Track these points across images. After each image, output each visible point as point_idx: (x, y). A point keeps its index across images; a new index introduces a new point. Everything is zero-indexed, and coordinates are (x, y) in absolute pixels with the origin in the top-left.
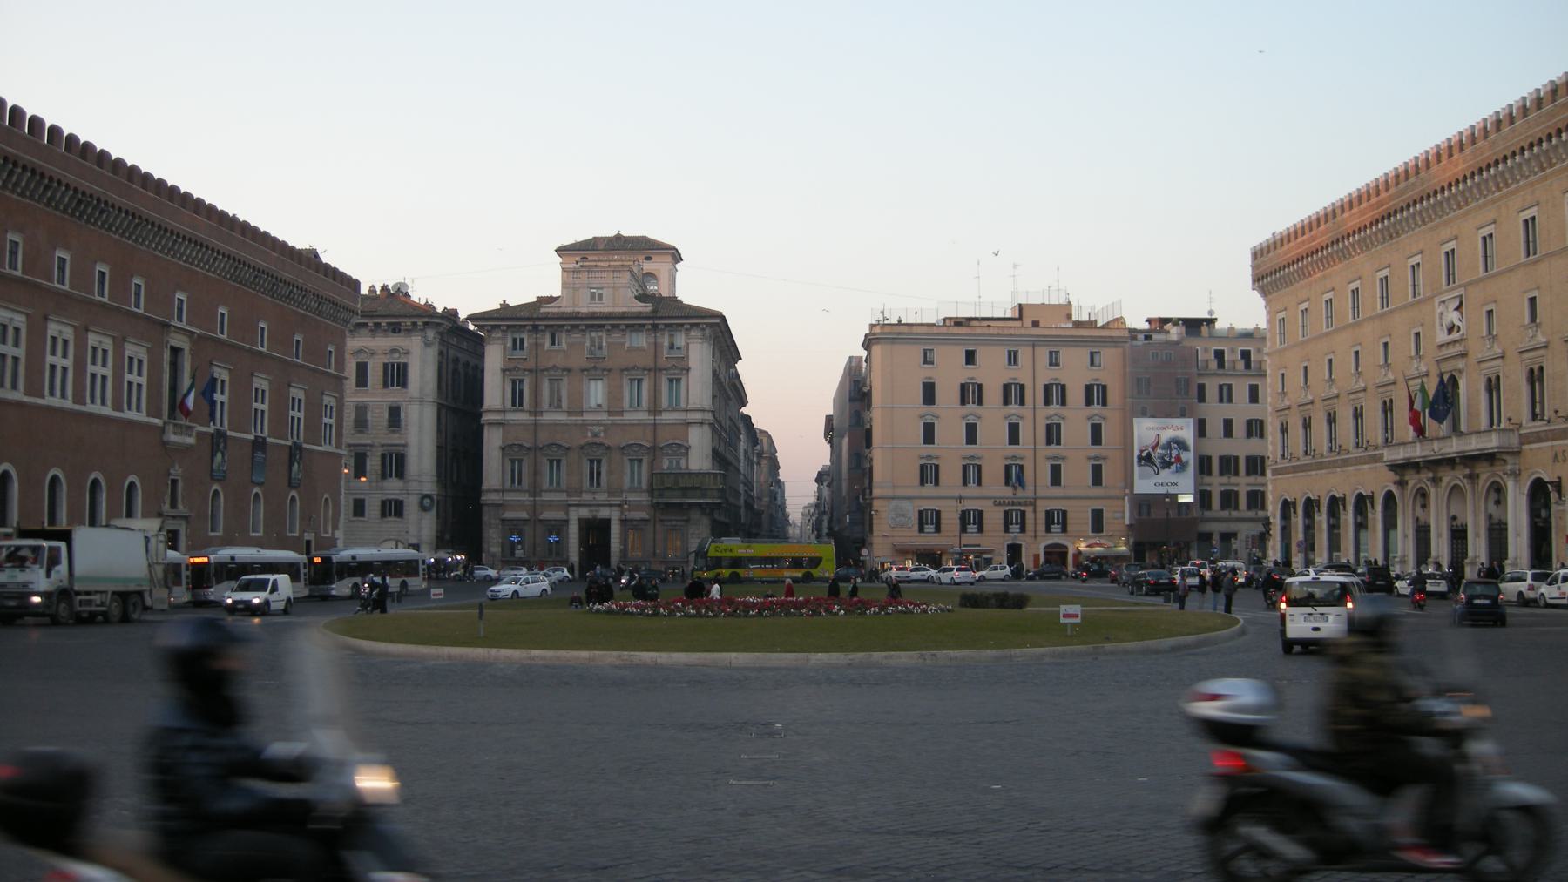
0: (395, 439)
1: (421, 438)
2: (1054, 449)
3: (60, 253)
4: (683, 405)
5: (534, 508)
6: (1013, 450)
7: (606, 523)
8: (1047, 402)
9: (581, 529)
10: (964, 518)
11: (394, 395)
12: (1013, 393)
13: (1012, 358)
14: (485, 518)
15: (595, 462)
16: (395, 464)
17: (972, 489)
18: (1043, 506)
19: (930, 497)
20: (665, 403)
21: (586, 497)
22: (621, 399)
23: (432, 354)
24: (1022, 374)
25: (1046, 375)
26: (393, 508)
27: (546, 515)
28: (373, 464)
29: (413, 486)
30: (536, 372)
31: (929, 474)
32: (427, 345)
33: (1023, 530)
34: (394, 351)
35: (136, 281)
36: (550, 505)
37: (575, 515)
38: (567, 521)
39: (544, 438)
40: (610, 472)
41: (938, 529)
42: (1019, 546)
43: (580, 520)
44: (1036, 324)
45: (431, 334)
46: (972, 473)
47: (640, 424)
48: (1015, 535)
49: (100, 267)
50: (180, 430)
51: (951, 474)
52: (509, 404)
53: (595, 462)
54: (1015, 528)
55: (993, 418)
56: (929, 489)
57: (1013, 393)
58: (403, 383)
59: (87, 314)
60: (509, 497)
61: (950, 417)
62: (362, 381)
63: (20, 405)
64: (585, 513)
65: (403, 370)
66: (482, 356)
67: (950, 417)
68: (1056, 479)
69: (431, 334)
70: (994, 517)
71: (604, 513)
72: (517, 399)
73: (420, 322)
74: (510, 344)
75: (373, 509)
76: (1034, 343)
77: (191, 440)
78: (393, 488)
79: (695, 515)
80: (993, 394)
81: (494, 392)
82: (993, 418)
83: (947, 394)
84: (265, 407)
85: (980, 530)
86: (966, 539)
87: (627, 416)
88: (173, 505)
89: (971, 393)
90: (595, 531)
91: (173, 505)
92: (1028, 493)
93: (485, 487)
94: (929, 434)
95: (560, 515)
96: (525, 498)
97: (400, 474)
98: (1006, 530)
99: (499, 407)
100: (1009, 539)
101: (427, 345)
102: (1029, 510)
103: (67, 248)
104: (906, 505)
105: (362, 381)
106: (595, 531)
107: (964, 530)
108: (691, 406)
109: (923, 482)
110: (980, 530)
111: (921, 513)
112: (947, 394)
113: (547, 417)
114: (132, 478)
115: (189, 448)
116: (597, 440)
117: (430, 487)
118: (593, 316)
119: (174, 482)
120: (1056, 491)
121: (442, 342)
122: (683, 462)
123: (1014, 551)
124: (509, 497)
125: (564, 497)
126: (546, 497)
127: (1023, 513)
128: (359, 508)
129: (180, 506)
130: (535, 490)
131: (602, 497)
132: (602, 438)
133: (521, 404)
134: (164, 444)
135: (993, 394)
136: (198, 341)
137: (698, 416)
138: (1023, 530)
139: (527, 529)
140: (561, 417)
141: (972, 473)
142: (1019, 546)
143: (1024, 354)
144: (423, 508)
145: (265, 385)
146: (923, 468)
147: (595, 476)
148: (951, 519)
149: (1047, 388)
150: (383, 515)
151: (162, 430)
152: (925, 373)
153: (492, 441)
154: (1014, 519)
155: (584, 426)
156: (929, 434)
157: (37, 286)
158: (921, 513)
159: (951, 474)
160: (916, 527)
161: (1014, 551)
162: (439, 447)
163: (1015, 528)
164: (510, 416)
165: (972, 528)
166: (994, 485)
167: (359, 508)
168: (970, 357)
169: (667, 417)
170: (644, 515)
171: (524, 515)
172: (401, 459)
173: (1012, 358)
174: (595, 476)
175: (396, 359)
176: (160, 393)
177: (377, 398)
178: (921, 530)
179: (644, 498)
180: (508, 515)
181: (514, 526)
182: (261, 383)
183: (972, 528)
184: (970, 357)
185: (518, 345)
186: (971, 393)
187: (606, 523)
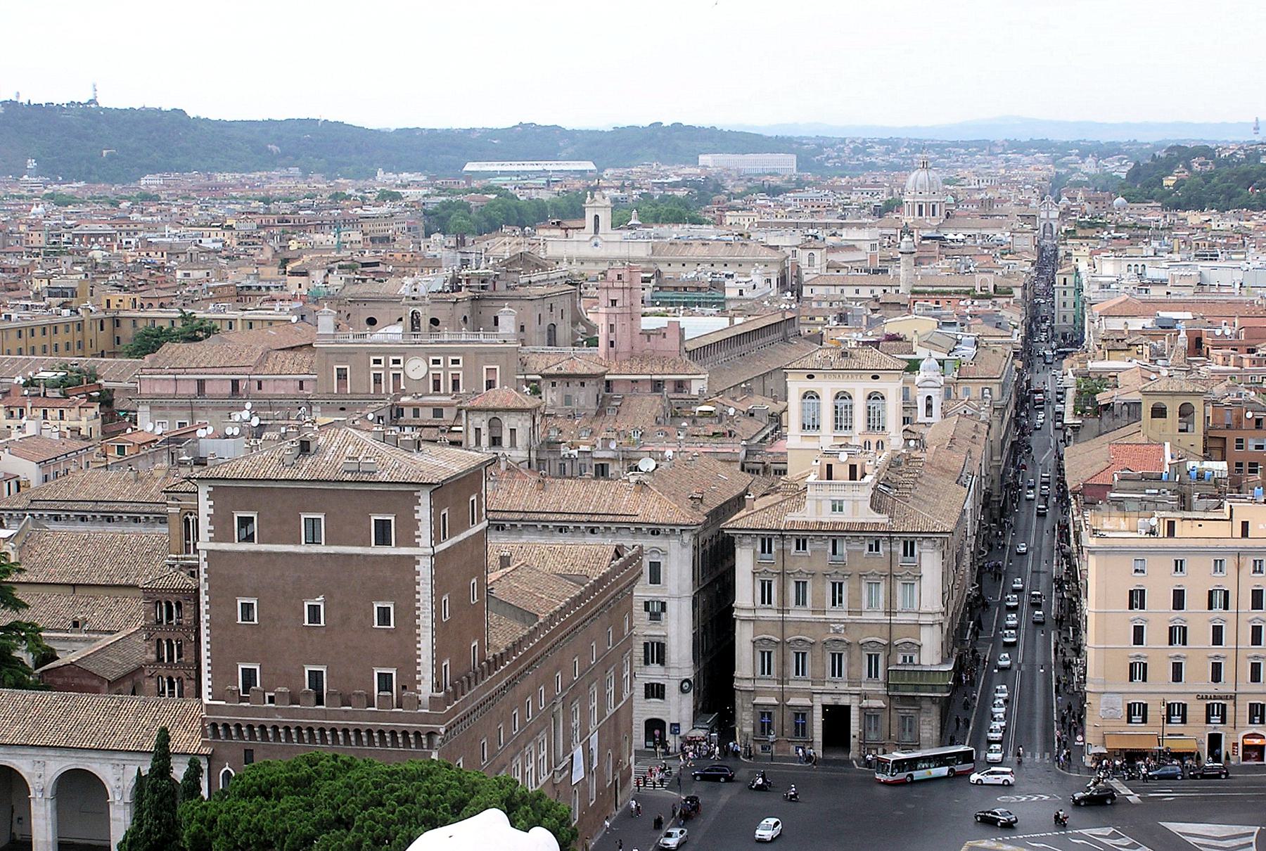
0: (654, 631)
1: (679, 631)
2: (1256, 650)
4: (916, 608)
5: (782, 696)
7: (847, 709)
9: (824, 714)
13: (1219, 565)
14: (738, 701)
15: (837, 659)
16: (656, 652)
19: (1138, 692)
21: (829, 687)
22: (860, 600)
23: (688, 554)
24: (1226, 581)
26: (654, 691)
29: (674, 673)
30: (783, 575)
31: (1138, 671)
32: (684, 546)
33: (1223, 721)
36: (796, 693)
40: (850, 665)
41: (1144, 721)
43: (824, 707)
45: (687, 537)
47: (878, 624)
48: (1216, 726)
52: (759, 601)
53: (837, 659)
54: (1216, 719)
56: (1138, 685)
57: (1218, 599)
60: (759, 684)
64: (828, 700)
67: (1158, 615)
68: (1256, 676)
69: (687, 537)
70: (1196, 710)
71: (844, 701)
72: (766, 597)
73: (678, 530)
74: (759, 549)
78: (654, 673)
79: (926, 705)
81: (745, 593)
82: (1198, 619)
85: (1184, 721)
86: (1170, 728)
87: (864, 616)
90: (837, 718)
92: (1225, 687)
93: (737, 674)
95: (806, 702)
96: (775, 685)
97: (661, 661)
98: (1208, 721)
99: (751, 605)
101: (684, 546)
102: (1229, 703)
104: (1119, 698)
106: (837, 718)
108: (923, 609)
110: (1184, 721)
111: (1129, 705)
113: (792, 615)
116: (837, 637)
117: (689, 674)
120: (1256, 687)
121: (696, 536)
122: (915, 660)
123: (1215, 740)
124: (759, 684)
125: (809, 685)
126: (792, 685)
127: (1224, 706)
131: (843, 687)
133: (770, 602)
137: (929, 619)
138: (1223, 721)
139: (777, 716)
140: (808, 616)
143: (1229, 563)
144: (683, 691)
147: (837, 670)
148: (1156, 711)
150: (647, 697)
152: (1135, 582)
153: (744, 637)
154: (1216, 710)
155: (826, 623)
158: (1129, 705)
161: (1215, 740)
163: (1216, 719)
164: (759, 613)
166: (1197, 680)
168: (1179, 566)
169: (899, 618)
170: (881, 704)
171: (774, 701)
172: (661, 648)
174: (837, 670)
178: (1129, 721)
179: (882, 689)
180: (759, 700)
181: (765, 718)
184: (1179, 566)
185: (766, 546)
187: (847, 709)
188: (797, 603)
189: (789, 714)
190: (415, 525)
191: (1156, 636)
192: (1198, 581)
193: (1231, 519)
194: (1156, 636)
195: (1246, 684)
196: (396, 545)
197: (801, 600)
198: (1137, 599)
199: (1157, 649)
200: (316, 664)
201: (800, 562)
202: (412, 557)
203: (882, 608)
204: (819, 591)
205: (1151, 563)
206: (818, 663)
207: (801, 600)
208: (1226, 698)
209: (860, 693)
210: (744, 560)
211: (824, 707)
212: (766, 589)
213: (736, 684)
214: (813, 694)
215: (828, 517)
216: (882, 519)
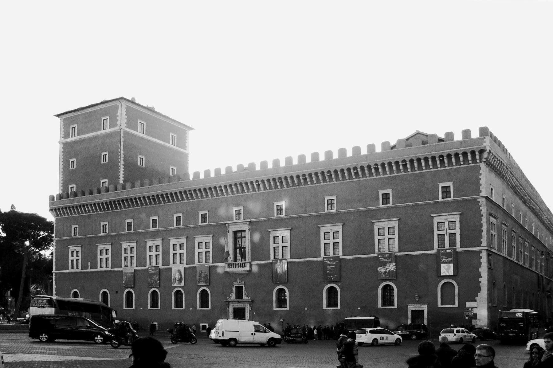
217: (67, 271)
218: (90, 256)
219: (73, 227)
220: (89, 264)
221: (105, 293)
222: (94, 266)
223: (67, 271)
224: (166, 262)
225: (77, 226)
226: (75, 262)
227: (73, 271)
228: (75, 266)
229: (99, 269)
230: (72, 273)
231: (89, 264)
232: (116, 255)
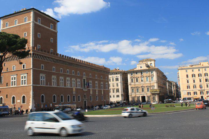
0: (118, 87)
3: (67, 70)
6: (194, 83)
8: (205, 76)
10: (194, 93)
11: (117, 82)
12: (200, 75)
13: (199, 70)
16: (118, 91)
17: (195, 89)
18: (206, 91)
19: (189, 90)
20: (151, 80)
21: (142, 93)
24: (201, 72)
25: (204, 72)
26: (118, 96)
27: (137, 96)
28: (115, 91)
31: (188, 87)
33: (203, 94)
34: (117, 76)
35: (78, 72)
36: (137, 94)
37: (141, 96)
38: (140, 97)
39: (136, 86)
42: (203, 96)
43: (142, 96)
44: (203, 65)
45: (121, 74)
46: (195, 87)
49: (73, 71)
50: (85, 89)
51: (192, 87)
55: (197, 79)
57: (200, 75)
58: (118, 80)
59: (71, 77)
61: (191, 79)
62: (113, 80)
63: (63, 88)
64: (142, 95)
65: (118, 79)
66: (127, 76)
67: (191, 79)
68: (207, 87)
70: (199, 93)
71: (144, 95)
72: (132, 81)
75: (116, 96)
76: (202, 68)
77: (87, 90)
78: (118, 94)
80: (197, 76)
82: (197, 79)
83: (190, 76)
84: (97, 85)
85: (197, 94)
88: (85, 98)
89: (193, 76)
91: (85, 98)
94: (188, 82)
95: (139, 96)
98: (201, 94)
100: (201, 95)
102: (204, 91)
103: (68, 69)
104: (186, 92)
105: (113, 80)
106: (143, 98)
107: (194, 95)
109: (188, 88)
110: (197, 94)
112: (190, 76)
114: (79, 95)
115: (87, 91)
118: (141, 70)
119: (85, 95)
120: (208, 88)
123: (202, 97)
127: (203, 92)
128: (114, 96)
129: (86, 98)
130: (135, 93)
131: (144, 93)
132: (143, 86)
134: (83, 91)
135: (197, 76)
136: (87, 78)
137: (156, 82)
138: (203, 94)
141: (195, 87)
142: (203, 96)
143: (201, 69)
145: (97, 83)
146: (187, 86)
149: (205, 74)
151: (83, 89)
155: (141, 84)
156: (188, 82)
157: (65, 74)
159: (192, 87)
160: (187, 95)
162: (123, 88)
165: (195, 94)
166: (198, 88)
167: (114, 96)
168: (193, 71)
171: (134, 96)
173: (199, 70)
175: (117, 77)
176: (82, 84)
177: (115, 82)
178: (188, 95)
179: (150, 93)
180: (132, 96)
182: (96, 82)
183: (195, 94)
184: (193, 71)
186: (193, 76)
187: (145, 96)
188: (137, 82)
189: (136, 98)
190: (30, 17)
191: (191, 81)
192: (196, 72)
193: (200, 64)
194: (191, 81)
195: (206, 88)
196: (28, 21)
197: (137, 81)
198: (187, 76)
199: (191, 84)
200: (65, 88)
201: (136, 75)
202: (30, 23)
203: (148, 81)
204: (139, 79)
205: (188, 70)
206: (140, 90)
207: (137, 81)
208: (203, 90)
209: (147, 94)
210: (129, 76)
211: (142, 96)
212: (132, 80)
213: (129, 94)
214: (140, 95)
215: (140, 69)
216: (148, 68)
217: (39, 85)
218: (49, 80)
219: (53, 67)
220: (49, 83)
221: (68, 96)
222: (51, 84)
223: (39, 85)
224: (71, 86)
225: (43, 65)
226: (43, 81)
227: (42, 85)
228: (43, 84)
229: (52, 86)
230: (41, 86)
231: (49, 83)
232: (58, 80)
